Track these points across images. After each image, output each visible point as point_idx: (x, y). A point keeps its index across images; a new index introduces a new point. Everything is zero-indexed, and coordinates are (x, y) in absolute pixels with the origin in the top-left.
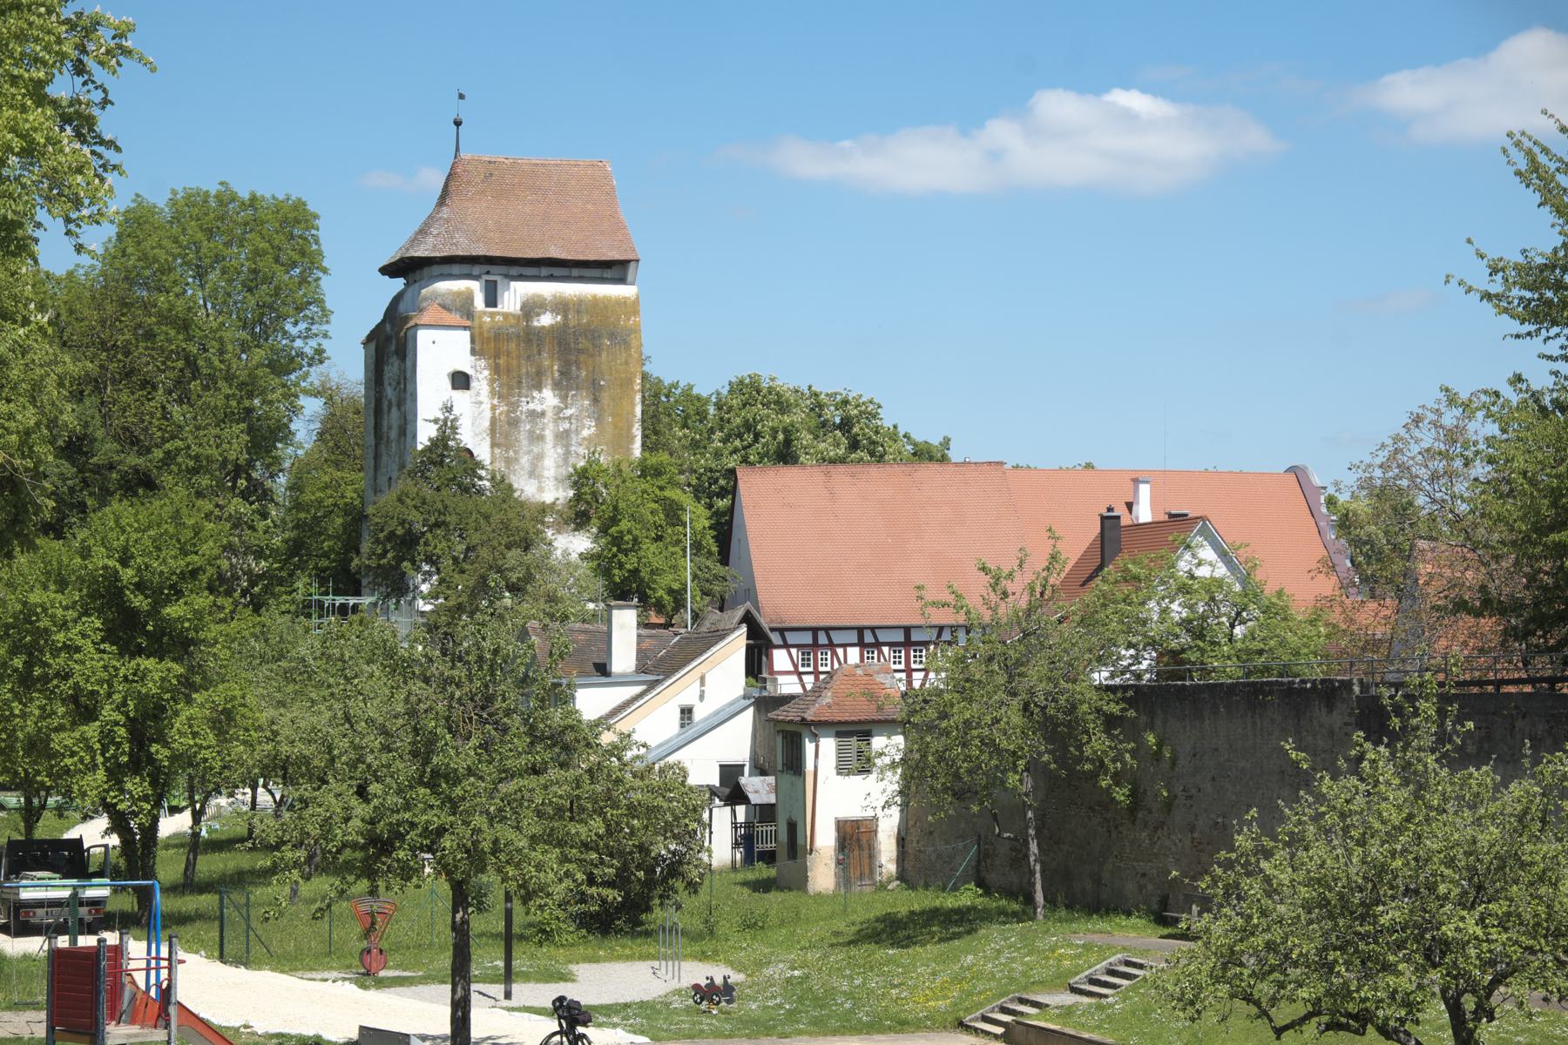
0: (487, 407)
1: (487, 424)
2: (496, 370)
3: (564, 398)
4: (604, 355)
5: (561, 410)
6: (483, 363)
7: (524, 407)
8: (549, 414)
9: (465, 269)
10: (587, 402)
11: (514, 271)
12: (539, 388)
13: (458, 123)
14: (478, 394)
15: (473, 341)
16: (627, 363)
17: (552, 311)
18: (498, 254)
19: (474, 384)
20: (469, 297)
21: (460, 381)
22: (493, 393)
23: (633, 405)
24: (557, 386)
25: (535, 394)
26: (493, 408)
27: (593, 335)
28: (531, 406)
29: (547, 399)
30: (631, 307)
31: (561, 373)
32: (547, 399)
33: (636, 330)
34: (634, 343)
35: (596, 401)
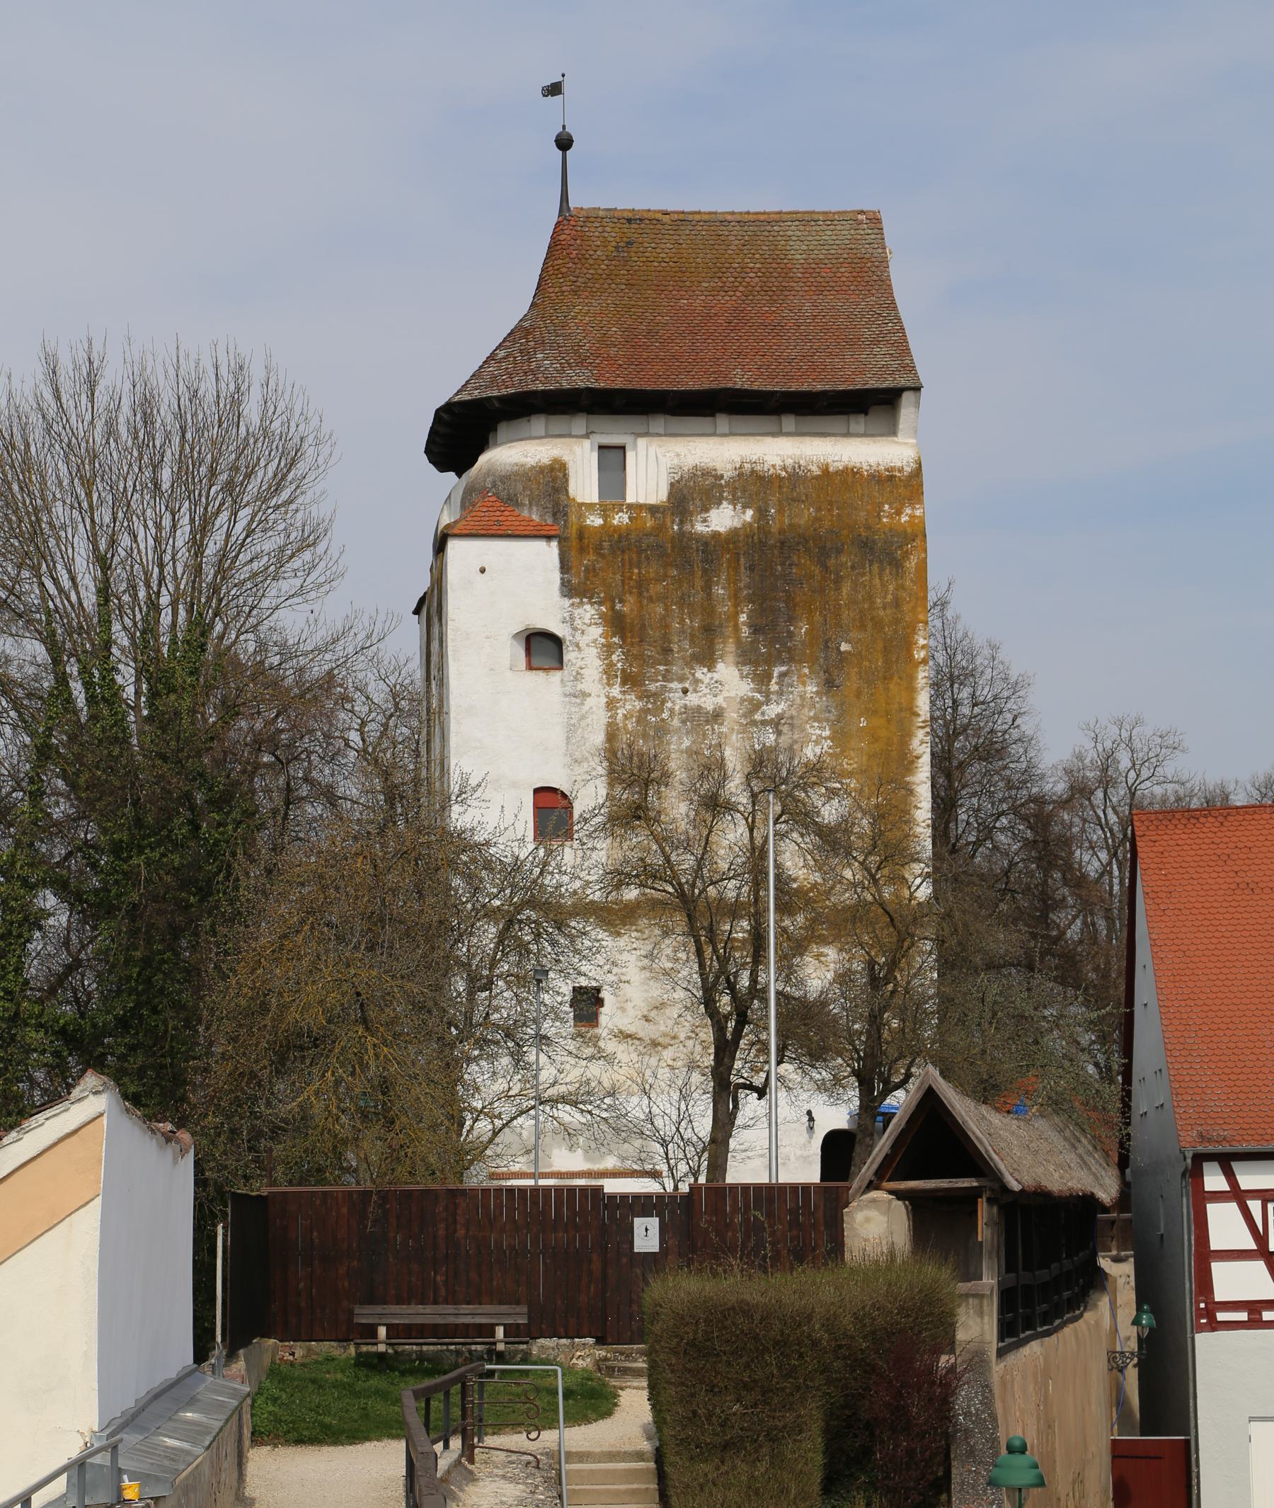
0: (596, 703)
1: (598, 738)
2: (616, 624)
3: (762, 680)
4: (846, 589)
5: (756, 706)
6: (588, 612)
7: (676, 701)
8: (732, 715)
9: (559, 423)
10: (811, 688)
11: (658, 423)
12: (707, 659)
13: (564, 143)
14: (578, 677)
15: (565, 567)
16: (897, 603)
17: (733, 502)
18: (619, 384)
19: (569, 655)
20: (555, 476)
21: (542, 647)
22: (609, 672)
23: (912, 690)
24: (747, 657)
25: (701, 672)
26: (611, 704)
27: (820, 546)
28: (693, 699)
29: (725, 684)
30: (905, 485)
31: (756, 629)
32: (725, 684)
33: (917, 534)
34: (911, 564)
35: (829, 685)
